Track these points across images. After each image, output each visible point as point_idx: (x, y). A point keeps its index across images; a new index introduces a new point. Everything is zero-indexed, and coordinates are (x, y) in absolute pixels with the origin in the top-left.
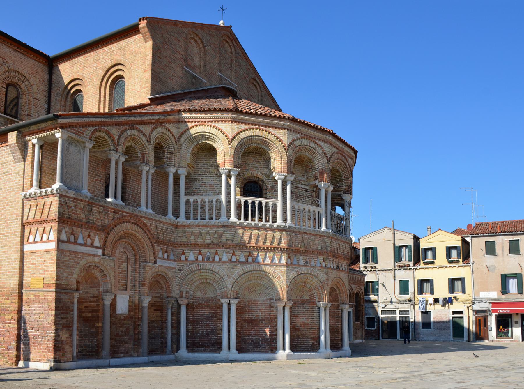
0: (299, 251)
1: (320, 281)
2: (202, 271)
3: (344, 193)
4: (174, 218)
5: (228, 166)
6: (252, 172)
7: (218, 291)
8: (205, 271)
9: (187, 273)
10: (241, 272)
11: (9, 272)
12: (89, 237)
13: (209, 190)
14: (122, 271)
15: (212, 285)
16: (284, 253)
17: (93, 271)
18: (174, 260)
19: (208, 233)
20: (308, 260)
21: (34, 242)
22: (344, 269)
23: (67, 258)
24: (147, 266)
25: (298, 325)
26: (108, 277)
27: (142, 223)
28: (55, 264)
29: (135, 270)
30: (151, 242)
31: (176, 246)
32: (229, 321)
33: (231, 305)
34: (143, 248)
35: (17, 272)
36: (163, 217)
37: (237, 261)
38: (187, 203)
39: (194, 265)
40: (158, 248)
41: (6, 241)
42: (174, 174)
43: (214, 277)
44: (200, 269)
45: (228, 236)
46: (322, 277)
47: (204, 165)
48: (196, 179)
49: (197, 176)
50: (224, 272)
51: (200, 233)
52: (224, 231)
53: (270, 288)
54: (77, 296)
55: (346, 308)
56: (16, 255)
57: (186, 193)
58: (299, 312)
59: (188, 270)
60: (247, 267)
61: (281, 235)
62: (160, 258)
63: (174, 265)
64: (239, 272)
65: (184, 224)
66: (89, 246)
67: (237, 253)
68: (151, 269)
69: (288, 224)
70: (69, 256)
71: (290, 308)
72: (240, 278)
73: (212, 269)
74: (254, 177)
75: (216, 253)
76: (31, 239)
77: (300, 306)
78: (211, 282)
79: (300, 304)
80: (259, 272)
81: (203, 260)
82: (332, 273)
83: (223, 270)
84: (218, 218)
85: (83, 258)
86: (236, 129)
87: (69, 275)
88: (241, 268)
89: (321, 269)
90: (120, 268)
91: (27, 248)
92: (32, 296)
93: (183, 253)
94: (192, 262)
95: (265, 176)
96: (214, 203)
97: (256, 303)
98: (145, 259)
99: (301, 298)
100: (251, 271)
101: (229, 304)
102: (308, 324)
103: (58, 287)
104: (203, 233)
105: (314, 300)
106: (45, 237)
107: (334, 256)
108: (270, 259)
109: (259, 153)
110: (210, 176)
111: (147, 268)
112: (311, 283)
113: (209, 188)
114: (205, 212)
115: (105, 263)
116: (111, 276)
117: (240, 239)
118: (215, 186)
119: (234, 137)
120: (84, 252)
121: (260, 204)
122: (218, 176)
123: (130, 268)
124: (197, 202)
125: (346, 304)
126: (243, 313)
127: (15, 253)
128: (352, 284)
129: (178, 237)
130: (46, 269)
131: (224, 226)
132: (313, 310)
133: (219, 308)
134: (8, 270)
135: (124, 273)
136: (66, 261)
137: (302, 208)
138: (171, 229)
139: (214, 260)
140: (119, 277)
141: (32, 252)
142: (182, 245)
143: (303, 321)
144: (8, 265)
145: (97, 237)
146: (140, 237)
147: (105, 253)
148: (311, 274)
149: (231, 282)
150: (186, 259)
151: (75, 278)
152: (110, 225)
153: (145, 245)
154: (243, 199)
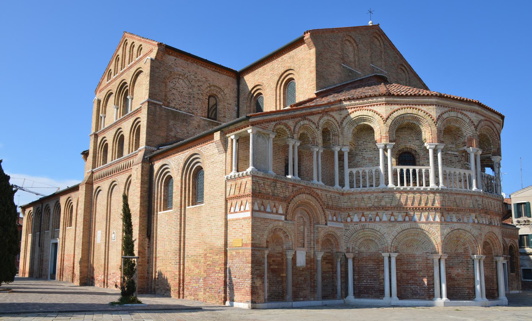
0: (452, 210)
1: (473, 235)
2: (365, 230)
3: (493, 156)
4: (340, 188)
5: (384, 141)
6: (406, 144)
7: (380, 247)
8: (368, 230)
9: (352, 232)
10: (400, 230)
11: (217, 235)
12: (275, 206)
13: (369, 163)
14: (300, 232)
15: (374, 241)
16: (437, 212)
17: (278, 233)
18: (342, 222)
19: (369, 198)
20: (460, 217)
21: (235, 212)
22: (496, 224)
23: (259, 224)
24: (320, 228)
25: (453, 275)
26: (289, 237)
27: (315, 194)
28: (251, 228)
29: (310, 231)
30: (322, 208)
31: (342, 210)
32: (390, 272)
33: (392, 258)
34: (316, 213)
35: (223, 235)
36: (331, 187)
37: (396, 221)
38: (351, 174)
39: (358, 225)
40: (328, 212)
41: (214, 212)
42: (339, 152)
43: (376, 234)
44: (363, 228)
45: (387, 200)
46: (475, 232)
47: (363, 142)
48: (357, 154)
49: (357, 152)
50: (384, 230)
51: (363, 198)
52: (383, 196)
53: (426, 243)
54: (267, 252)
55: (501, 260)
56: (222, 223)
57: (350, 167)
58: (453, 264)
59: (353, 230)
60: (404, 225)
61: (434, 197)
62: (330, 221)
63: (342, 225)
64: (397, 230)
65: (348, 192)
66: (274, 214)
67: (395, 214)
68: (323, 230)
69: (440, 187)
70: (260, 222)
71: (446, 260)
72: (399, 235)
73: (374, 228)
74: (407, 148)
75: (377, 215)
76: (232, 210)
77: (455, 259)
78: (374, 239)
79: (455, 257)
80: (416, 229)
81: (366, 220)
82: (484, 228)
83: (384, 228)
84: (377, 185)
85: (271, 223)
89: (474, 225)
90: (299, 230)
91: (230, 217)
92: (234, 253)
93: (349, 216)
94: (357, 223)
95: (417, 147)
96: (374, 173)
97: (413, 256)
98: (318, 222)
99: (455, 251)
100: (409, 229)
101: (390, 257)
102: (463, 275)
103: (253, 245)
104: (365, 198)
105: (468, 253)
106: (242, 207)
107: (486, 213)
108: (425, 218)
109: (411, 128)
110: (369, 150)
111: (320, 229)
112: (465, 237)
113: (369, 161)
114: (366, 181)
115: (287, 227)
116: (292, 237)
117: (397, 202)
118: (373, 158)
120: (271, 218)
121: (414, 171)
122: (376, 150)
123: (306, 230)
124: (359, 173)
125: (500, 256)
126: (402, 265)
127: (221, 221)
128: (505, 237)
129: (344, 202)
130: (244, 232)
131: (383, 192)
132: (468, 262)
133: (381, 261)
134: (216, 233)
135: (302, 234)
136: (258, 226)
137: (452, 172)
138: (338, 197)
139: (375, 220)
140: (298, 237)
141: (233, 220)
142: (348, 209)
143: (458, 272)
144: (216, 230)
145: (280, 206)
146: (314, 204)
147: (287, 219)
148: (464, 230)
149: (391, 239)
150: (352, 221)
151: (265, 238)
152: (290, 196)
153: (318, 211)
154: (399, 168)
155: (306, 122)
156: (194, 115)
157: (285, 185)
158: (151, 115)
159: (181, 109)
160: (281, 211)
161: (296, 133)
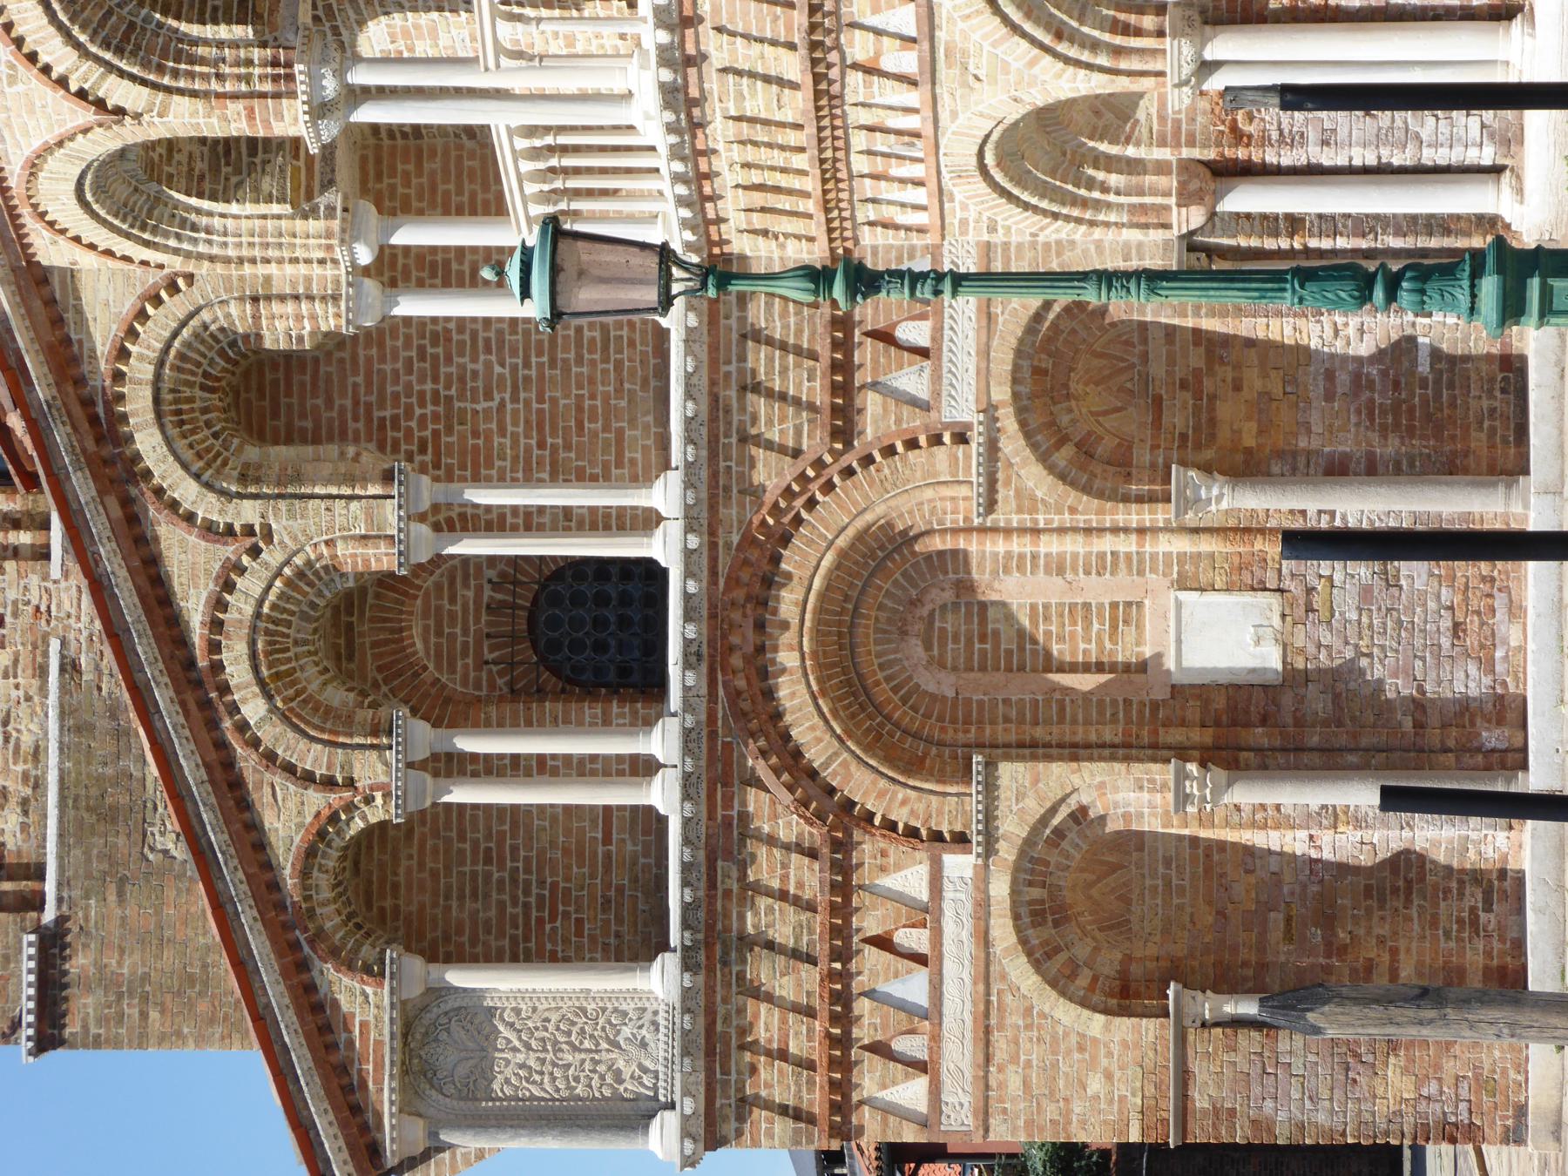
23: (1014, 1082)
62: (937, 394)
85: (1004, 977)
86: (20, 87)
87: (1092, 1064)
88: (961, 25)
119: (82, 94)
151: (1107, 1028)
155: (237, 671)
156: (55, 645)
157: (728, 855)
158: (144, 1015)
159: (27, 741)
160: (911, 879)
161: (347, 765)
